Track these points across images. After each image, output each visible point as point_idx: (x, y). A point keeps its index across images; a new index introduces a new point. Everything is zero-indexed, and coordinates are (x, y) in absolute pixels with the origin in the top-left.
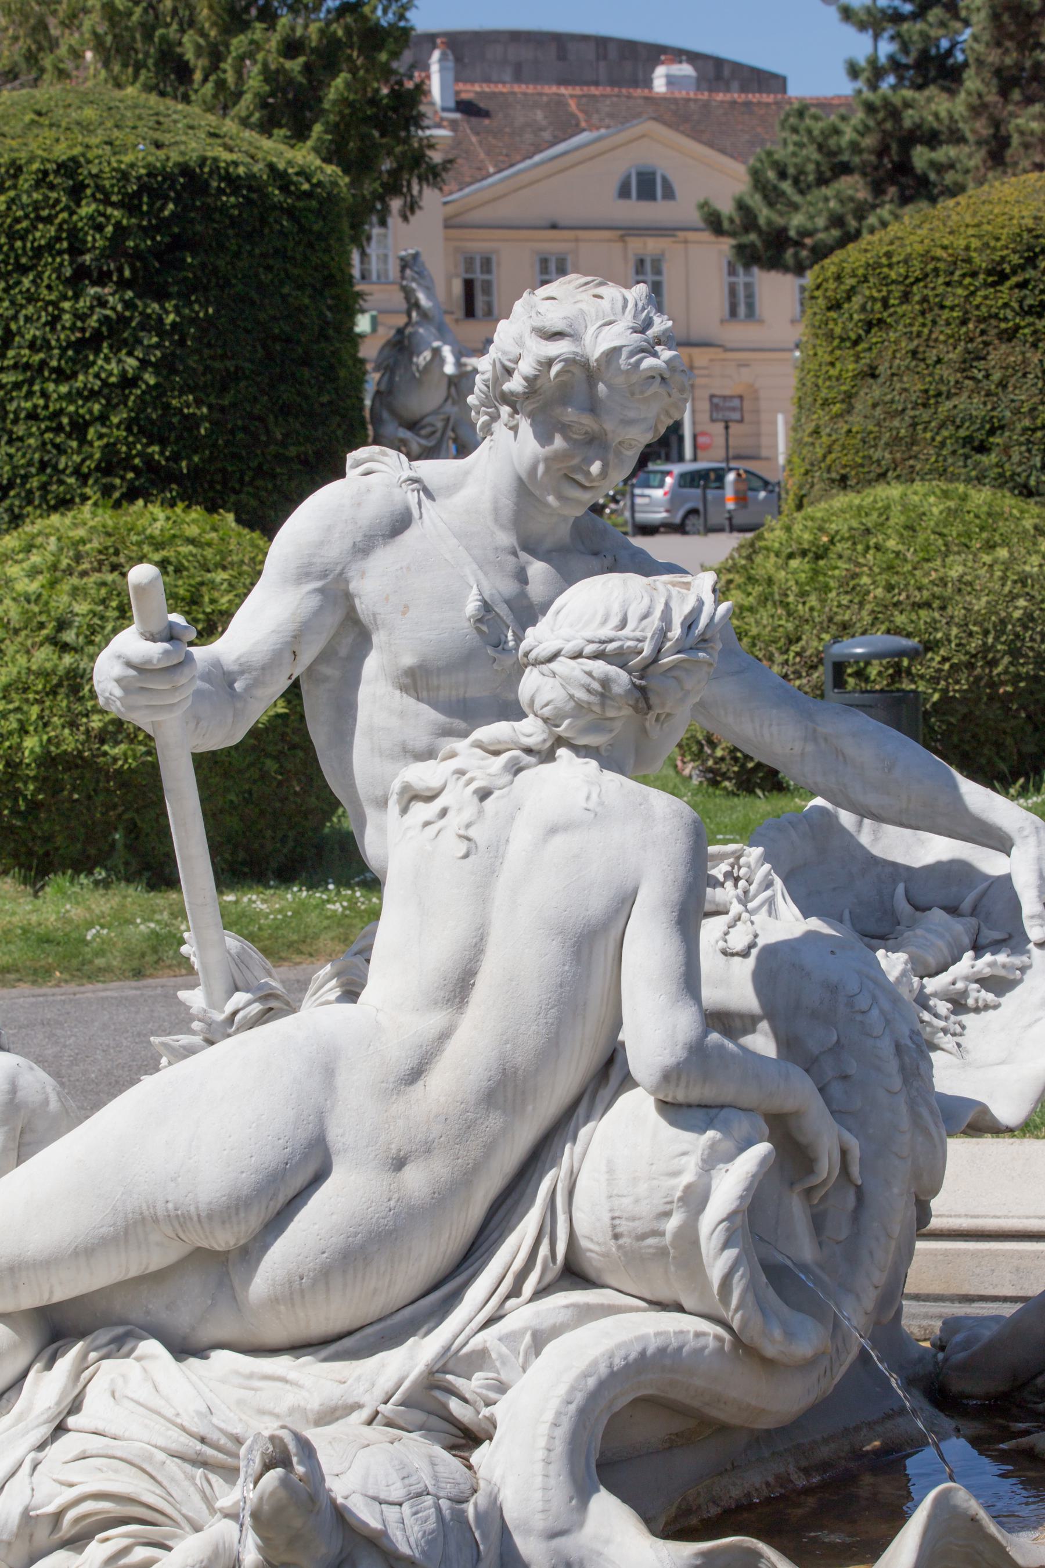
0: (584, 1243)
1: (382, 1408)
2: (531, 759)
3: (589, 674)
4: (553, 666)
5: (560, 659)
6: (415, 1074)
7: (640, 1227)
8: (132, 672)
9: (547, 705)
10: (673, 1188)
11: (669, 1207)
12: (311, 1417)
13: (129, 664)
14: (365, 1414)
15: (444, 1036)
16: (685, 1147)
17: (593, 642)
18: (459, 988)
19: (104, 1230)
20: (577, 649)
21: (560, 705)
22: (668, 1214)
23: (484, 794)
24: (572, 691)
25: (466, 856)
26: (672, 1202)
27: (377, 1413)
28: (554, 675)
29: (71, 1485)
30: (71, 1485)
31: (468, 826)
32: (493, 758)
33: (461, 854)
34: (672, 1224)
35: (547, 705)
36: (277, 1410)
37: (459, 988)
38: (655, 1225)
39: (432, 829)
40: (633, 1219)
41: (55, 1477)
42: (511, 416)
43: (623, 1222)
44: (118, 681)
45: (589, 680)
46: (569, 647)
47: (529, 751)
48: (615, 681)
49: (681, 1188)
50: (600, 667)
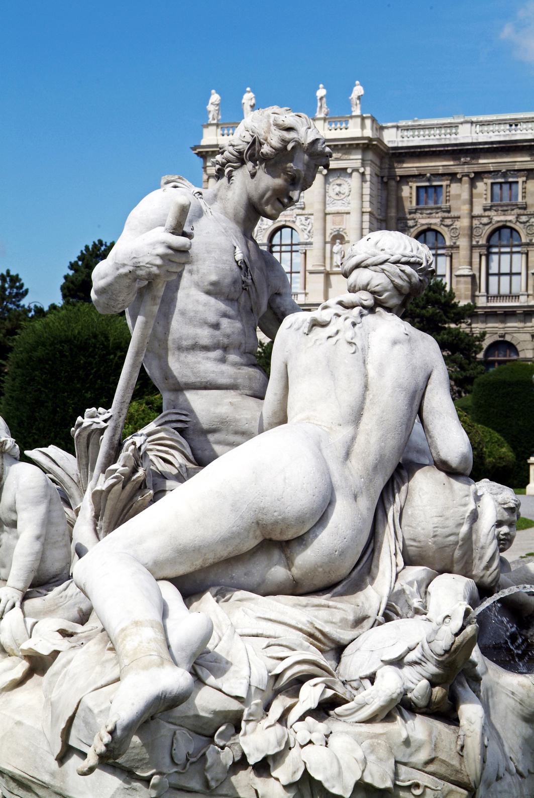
0: (408, 542)
1: (377, 618)
2: (365, 312)
3: (403, 271)
4: (383, 266)
5: (387, 263)
6: (348, 455)
7: (447, 531)
8: (170, 252)
9: (377, 286)
10: (466, 512)
11: (462, 521)
12: (350, 623)
13: (170, 247)
14: (371, 621)
15: (354, 439)
16: (466, 493)
17: (405, 256)
18: (357, 416)
19: (234, 529)
20: (398, 259)
21: (384, 285)
22: (461, 525)
23: (354, 324)
24: (393, 279)
25: (354, 353)
26: (464, 519)
27: (376, 620)
28: (383, 271)
29: (282, 659)
30: (282, 659)
31: (352, 339)
32: (347, 311)
33: (352, 352)
34: (465, 529)
35: (377, 286)
36: (334, 620)
37: (357, 416)
38: (455, 530)
39: (334, 340)
40: (444, 527)
41: (268, 655)
42: (254, 167)
43: (439, 529)
44: (162, 257)
45: (401, 274)
46: (393, 259)
47: (364, 307)
48: (414, 276)
49: (469, 511)
50: (408, 269)
